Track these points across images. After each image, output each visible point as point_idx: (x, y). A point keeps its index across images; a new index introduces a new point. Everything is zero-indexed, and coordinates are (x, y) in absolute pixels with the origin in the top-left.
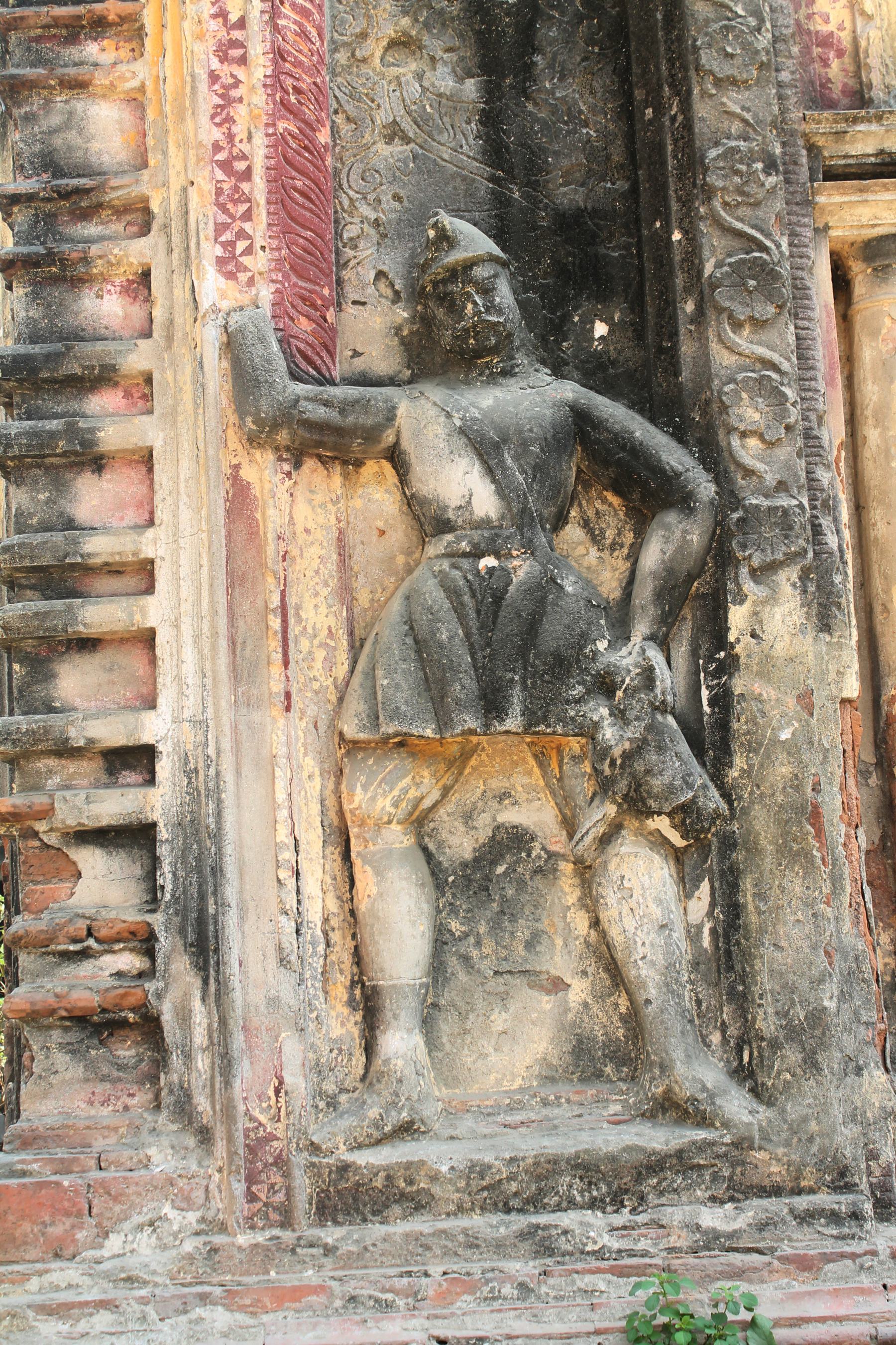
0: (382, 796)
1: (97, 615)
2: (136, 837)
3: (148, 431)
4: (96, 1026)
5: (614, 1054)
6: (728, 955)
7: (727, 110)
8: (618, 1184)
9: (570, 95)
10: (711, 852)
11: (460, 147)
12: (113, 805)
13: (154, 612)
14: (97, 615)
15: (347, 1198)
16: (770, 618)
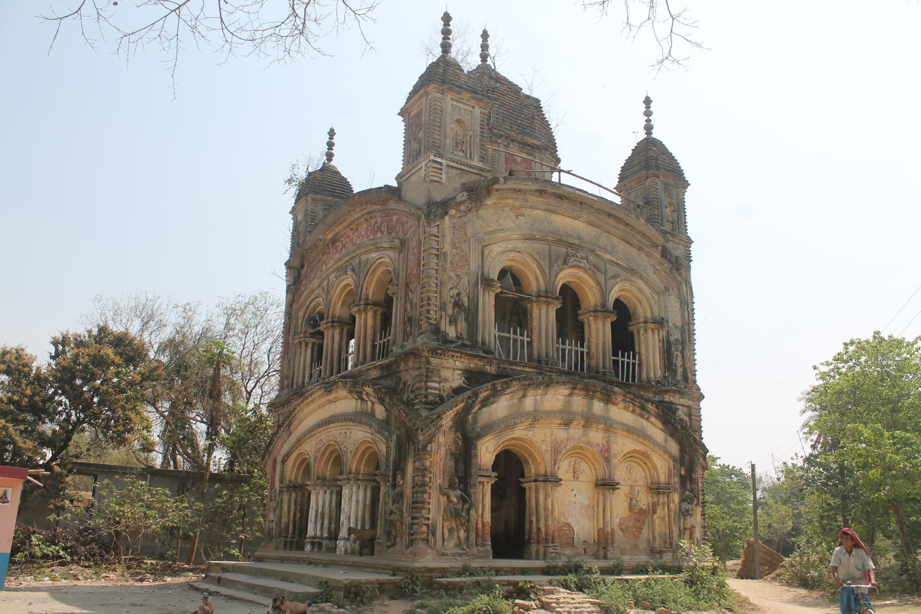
0: (446, 524)
1: (427, 506)
2: (428, 525)
3: (431, 491)
4: (423, 540)
5: (459, 545)
6: (467, 538)
7: (473, 470)
8: (460, 555)
9: (461, 465)
10: (467, 531)
11: (453, 470)
12: (427, 522)
13: (430, 506)
14: (427, 506)
15: (443, 555)
16: (472, 512)
